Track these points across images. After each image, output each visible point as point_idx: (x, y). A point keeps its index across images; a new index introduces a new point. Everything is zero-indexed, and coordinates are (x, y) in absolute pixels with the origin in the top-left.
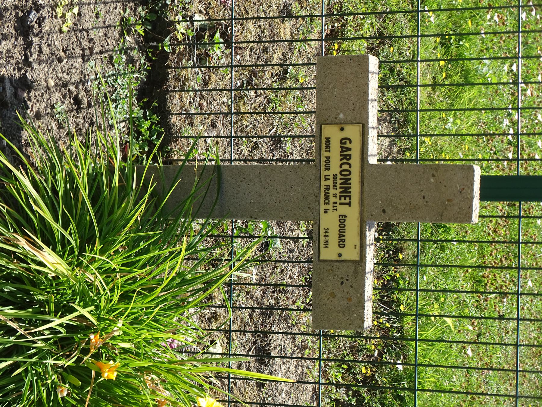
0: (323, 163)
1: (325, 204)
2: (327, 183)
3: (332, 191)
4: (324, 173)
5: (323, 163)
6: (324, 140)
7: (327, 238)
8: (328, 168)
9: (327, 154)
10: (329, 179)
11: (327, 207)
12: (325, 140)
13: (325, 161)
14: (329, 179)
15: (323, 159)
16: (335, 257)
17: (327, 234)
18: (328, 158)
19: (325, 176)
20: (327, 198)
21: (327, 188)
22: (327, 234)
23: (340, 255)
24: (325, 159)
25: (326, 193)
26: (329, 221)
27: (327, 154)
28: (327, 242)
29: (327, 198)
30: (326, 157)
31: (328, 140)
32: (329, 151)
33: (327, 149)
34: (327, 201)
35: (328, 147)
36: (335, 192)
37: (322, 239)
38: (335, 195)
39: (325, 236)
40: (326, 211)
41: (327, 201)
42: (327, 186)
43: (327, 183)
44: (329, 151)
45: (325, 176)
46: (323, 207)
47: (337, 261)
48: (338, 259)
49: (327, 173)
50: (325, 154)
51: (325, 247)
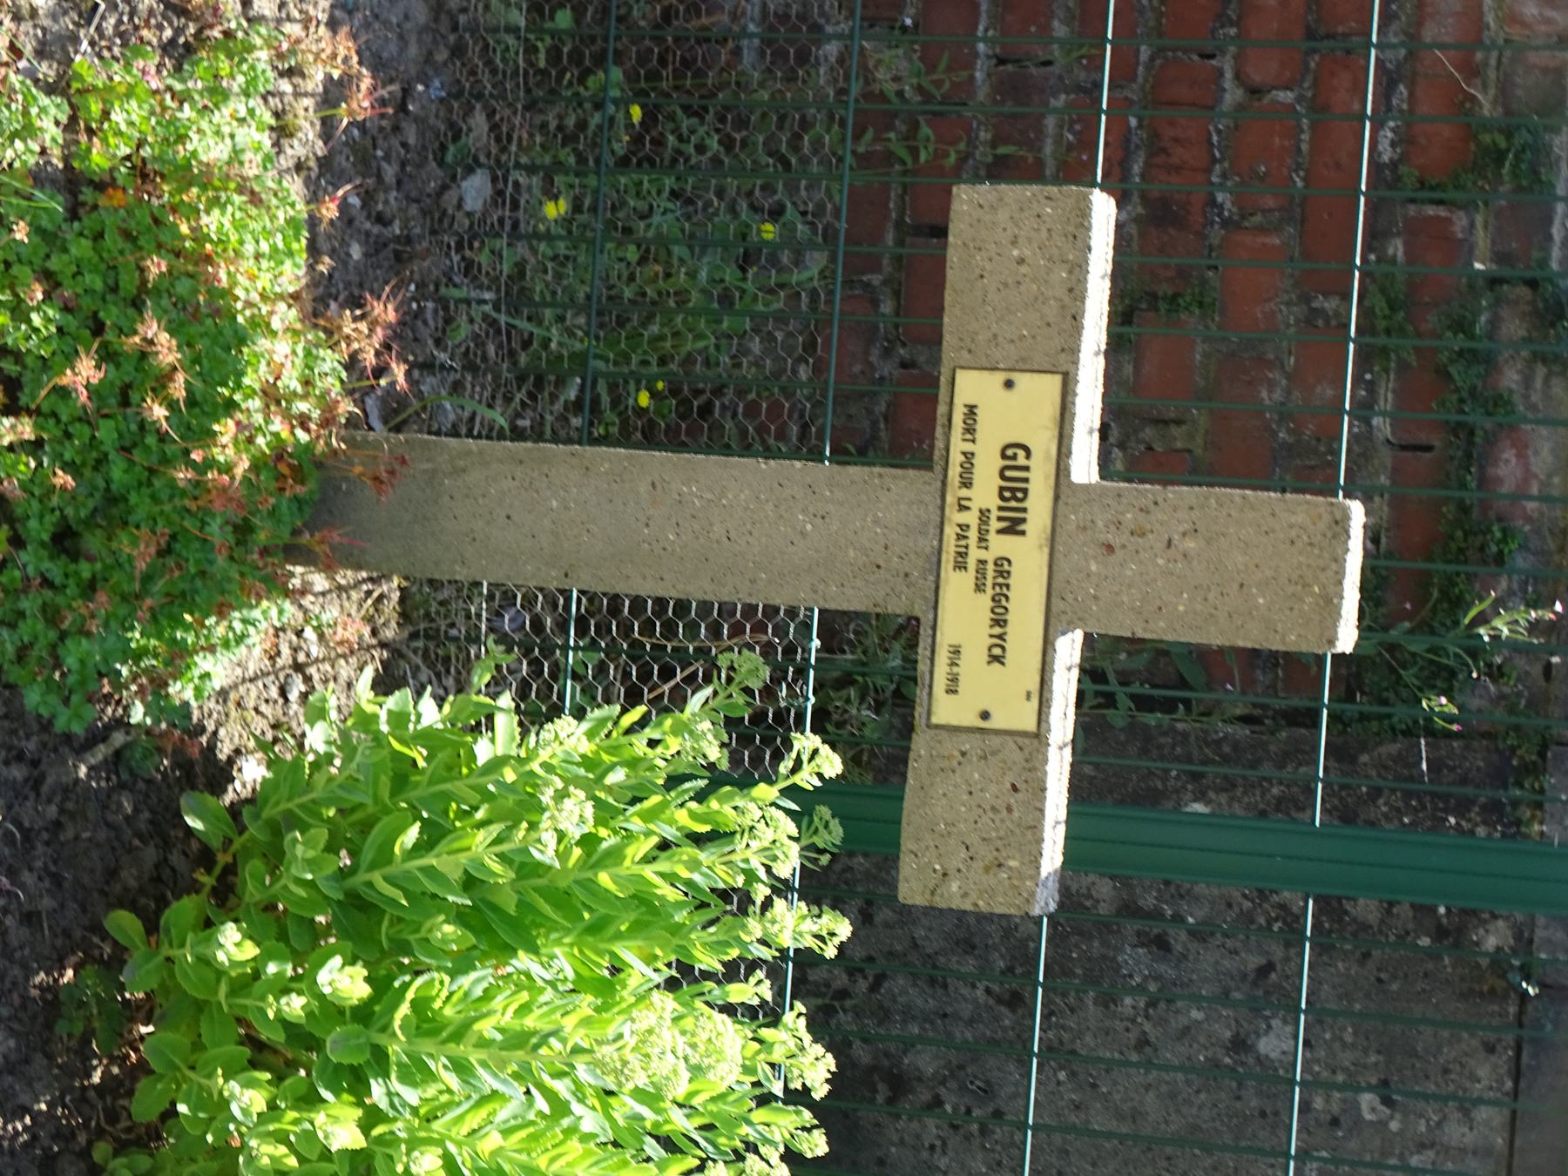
5: (954, 472)
7: (955, 669)
8: (967, 483)
9: (969, 447)
15: (956, 458)
16: (972, 720)
18: (968, 456)
23: (985, 715)
24: (963, 458)
27: (969, 447)
28: (954, 679)
30: (964, 454)
31: (971, 410)
32: (973, 441)
33: (968, 436)
35: (970, 430)
39: (953, 664)
44: (973, 441)
47: (981, 730)
50: (958, 445)
51: (951, 691)
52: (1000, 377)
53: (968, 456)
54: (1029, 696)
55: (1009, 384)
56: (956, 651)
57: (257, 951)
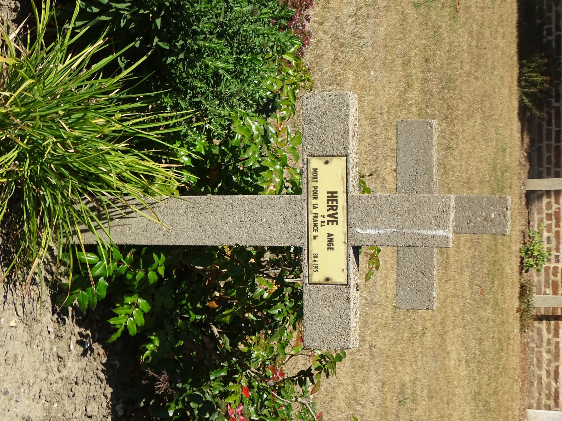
0: (311, 194)
2: (315, 211)
3: (320, 219)
4: (312, 201)
5: (311, 194)
6: (311, 171)
7: (316, 263)
8: (316, 198)
10: (317, 208)
11: (315, 233)
12: (313, 171)
14: (317, 208)
15: (311, 189)
17: (316, 259)
21: (316, 216)
23: (328, 279)
25: (315, 221)
28: (316, 267)
29: (316, 225)
31: (315, 170)
32: (317, 181)
33: (315, 180)
35: (315, 177)
36: (322, 219)
38: (323, 222)
40: (315, 238)
42: (315, 214)
43: (315, 211)
46: (312, 234)
49: (314, 201)
50: (312, 184)
54: (343, 270)
56: (316, 256)
57: (151, 282)
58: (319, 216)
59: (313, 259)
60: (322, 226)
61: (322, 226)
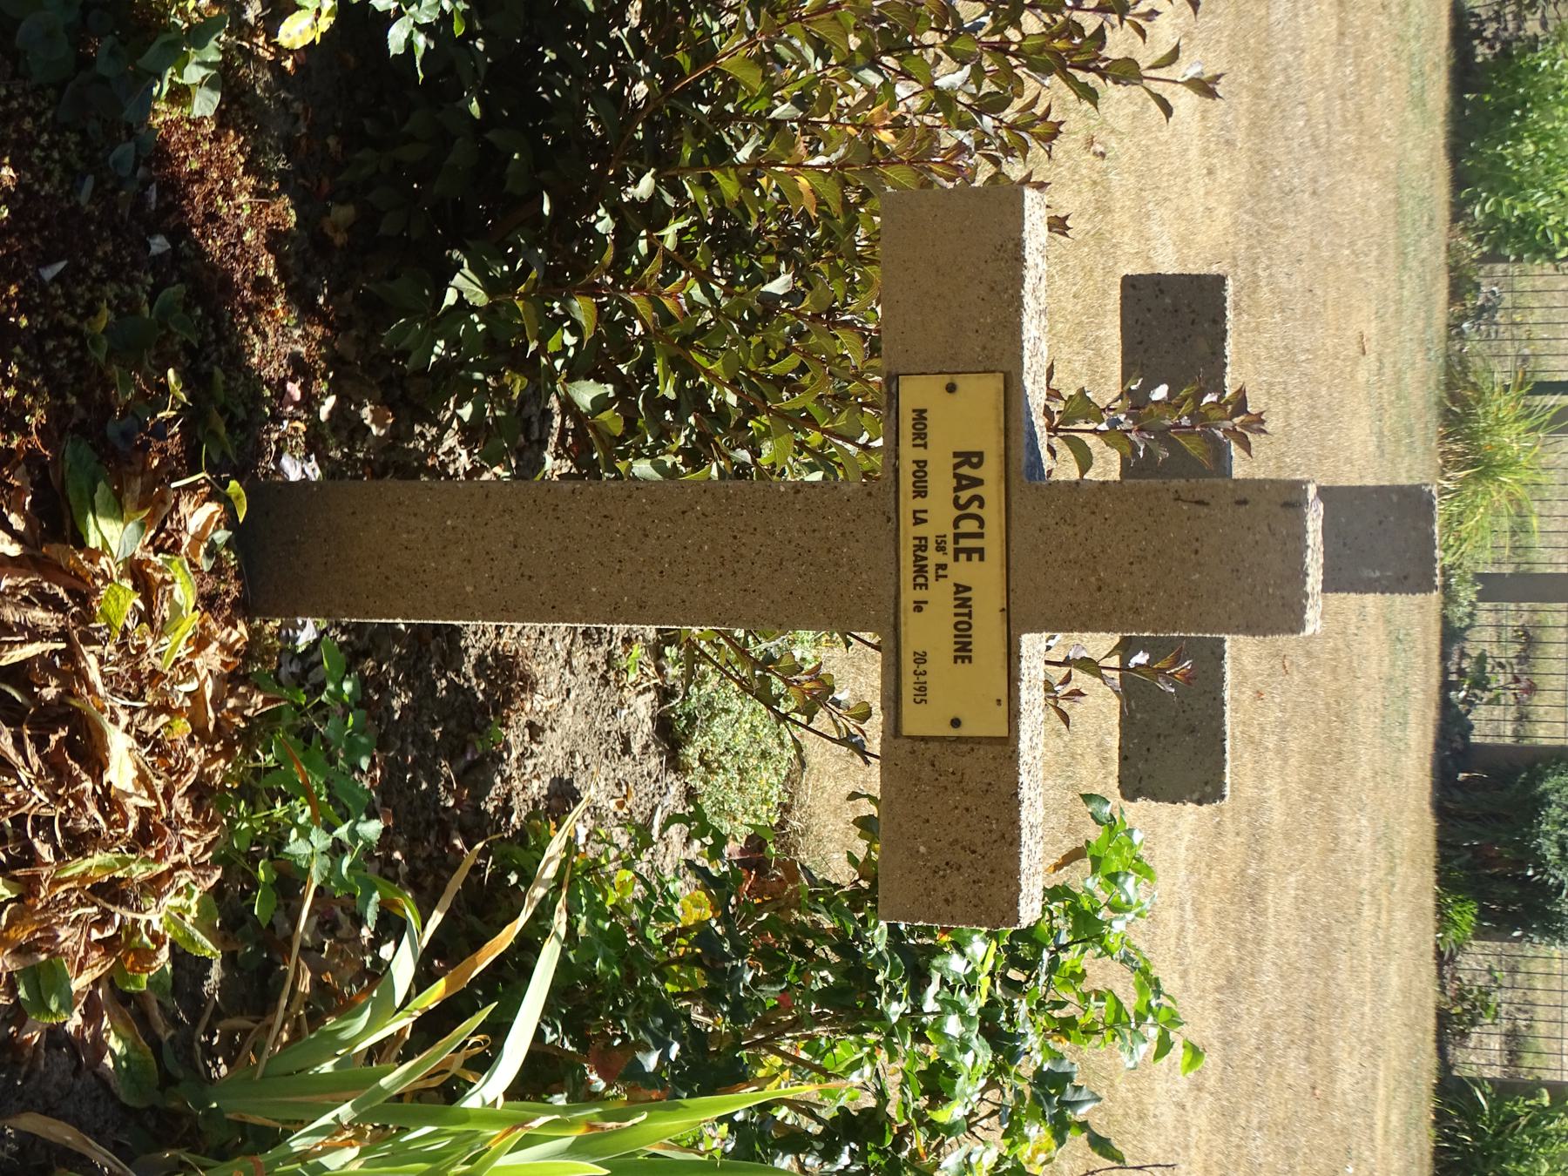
1: (915, 586)
2: (921, 530)
4: (908, 504)
7: (922, 679)
8: (921, 493)
9: (920, 454)
10: (925, 521)
11: (920, 594)
13: (914, 474)
14: (925, 521)
18: (921, 465)
19: (915, 512)
20: (921, 570)
22: (922, 668)
23: (956, 723)
24: (915, 467)
25: (917, 559)
26: (929, 630)
27: (920, 454)
28: (922, 689)
29: (921, 570)
31: (920, 415)
32: (925, 446)
33: (919, 442)
34: (921, 580)
35: (920, 435)
37: (908, 681)
40: (919, 607)
41: (921, 580)
42: (920, 539)
43: (921, 530)
44: (925, 446)
45: (915, 512)
46: (909, 596)
48: (954, 732)
49: (919, 503)
52: (946, 379)
53: (921, 465)
55: (951, 388)
56: (921, 658)
58: (932, 545)
59: (914, 666)
60: (938, 577)
61: (938, 577)
